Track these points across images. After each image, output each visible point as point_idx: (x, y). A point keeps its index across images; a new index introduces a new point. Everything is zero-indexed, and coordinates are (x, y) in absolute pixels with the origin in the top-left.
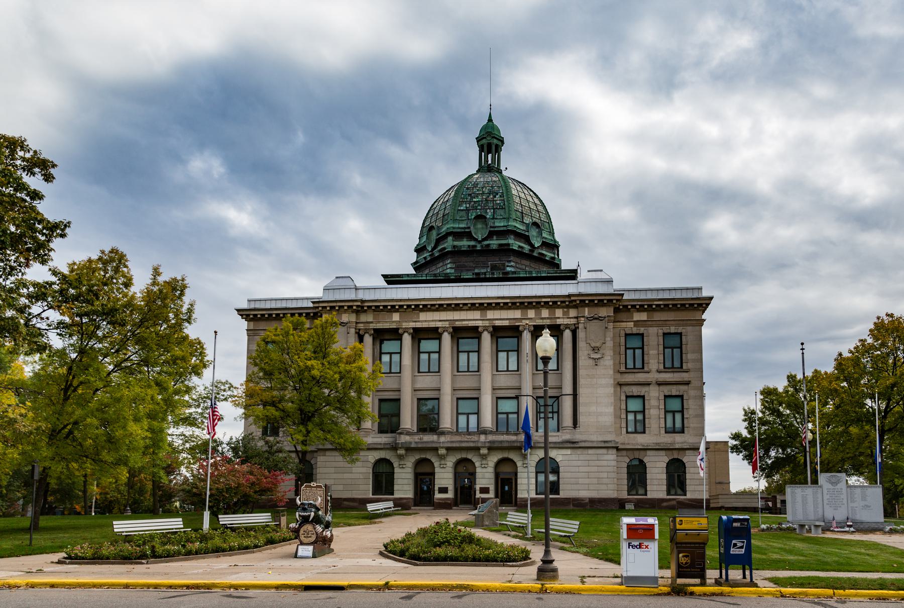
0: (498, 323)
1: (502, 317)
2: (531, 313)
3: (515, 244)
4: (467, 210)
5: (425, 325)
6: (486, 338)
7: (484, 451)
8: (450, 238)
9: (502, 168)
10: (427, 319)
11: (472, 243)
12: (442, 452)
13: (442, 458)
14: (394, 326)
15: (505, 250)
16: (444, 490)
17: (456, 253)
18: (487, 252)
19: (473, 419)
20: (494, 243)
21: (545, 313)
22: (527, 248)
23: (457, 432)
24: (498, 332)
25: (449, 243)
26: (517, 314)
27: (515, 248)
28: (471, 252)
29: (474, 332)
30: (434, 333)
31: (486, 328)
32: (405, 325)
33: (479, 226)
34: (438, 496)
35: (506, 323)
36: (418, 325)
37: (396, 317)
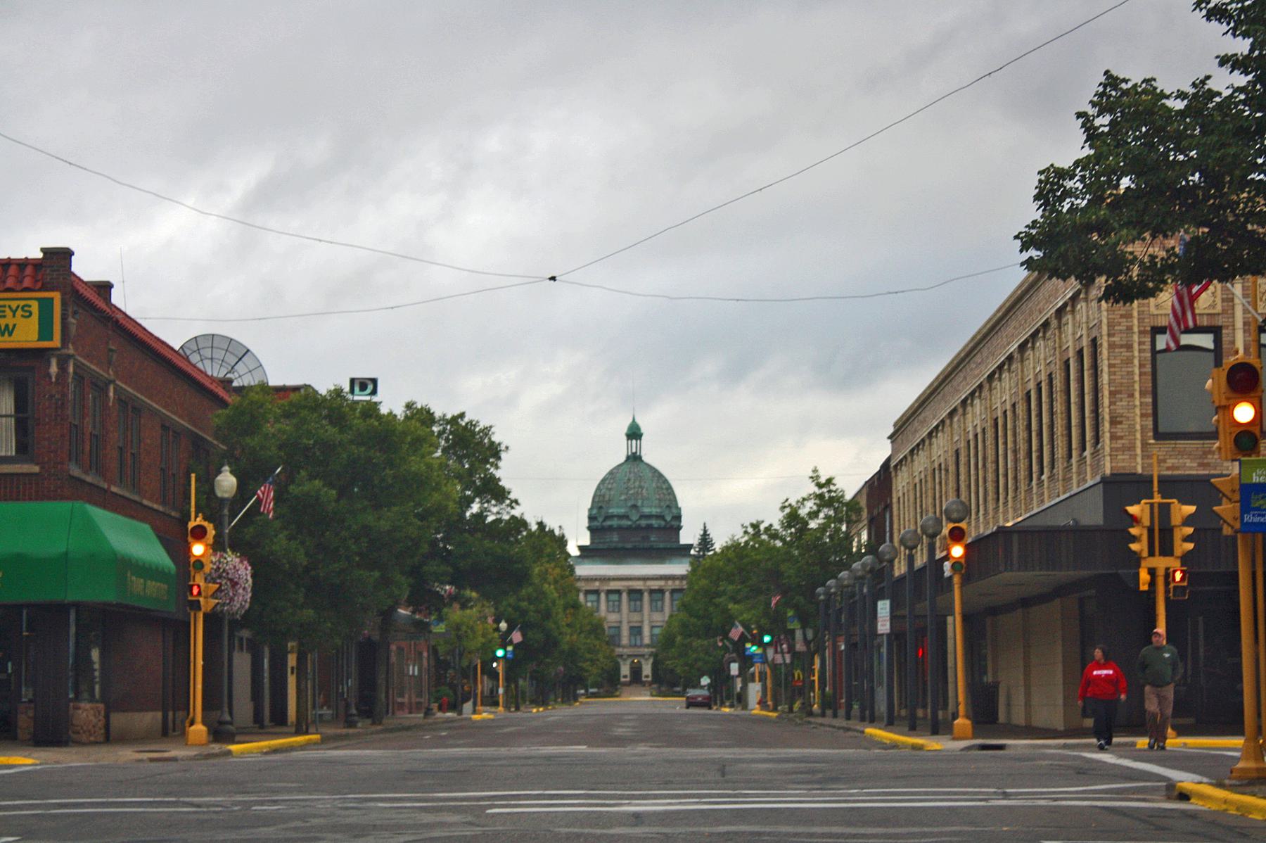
0: (653, 588)
1: (655, 585)
2: (670, 582)
3: (654, 522)
4: (626, 500)
5: (613, 588)
6: (646, 595)
7: (647, 657)
8: (616, 519)
9: (643, 454)
10: (614, 585)
11: (629, 523)
12: (625, 657)
13: (625, 660)
14: (595, 588)
15: (649, 527)
16: (625, 677)
17: (620, 528)
18: (639, 528)
19: (638, 638)
20: (643, 523)
21: (677, 582)
22: (663, 523)
23: (631, 646)
24: (652, 592)
25: (615, 522)
26: (662, 583)
27: (656, 526)
28: (629, 528)
29: (640, 592)
30: (618, 592)
31: (646, 590)
32: (601, 588)
33: (634, 511)
34: (623, 680)
35: (656, 588)
36: (609, 588)
37: (597, 584)
